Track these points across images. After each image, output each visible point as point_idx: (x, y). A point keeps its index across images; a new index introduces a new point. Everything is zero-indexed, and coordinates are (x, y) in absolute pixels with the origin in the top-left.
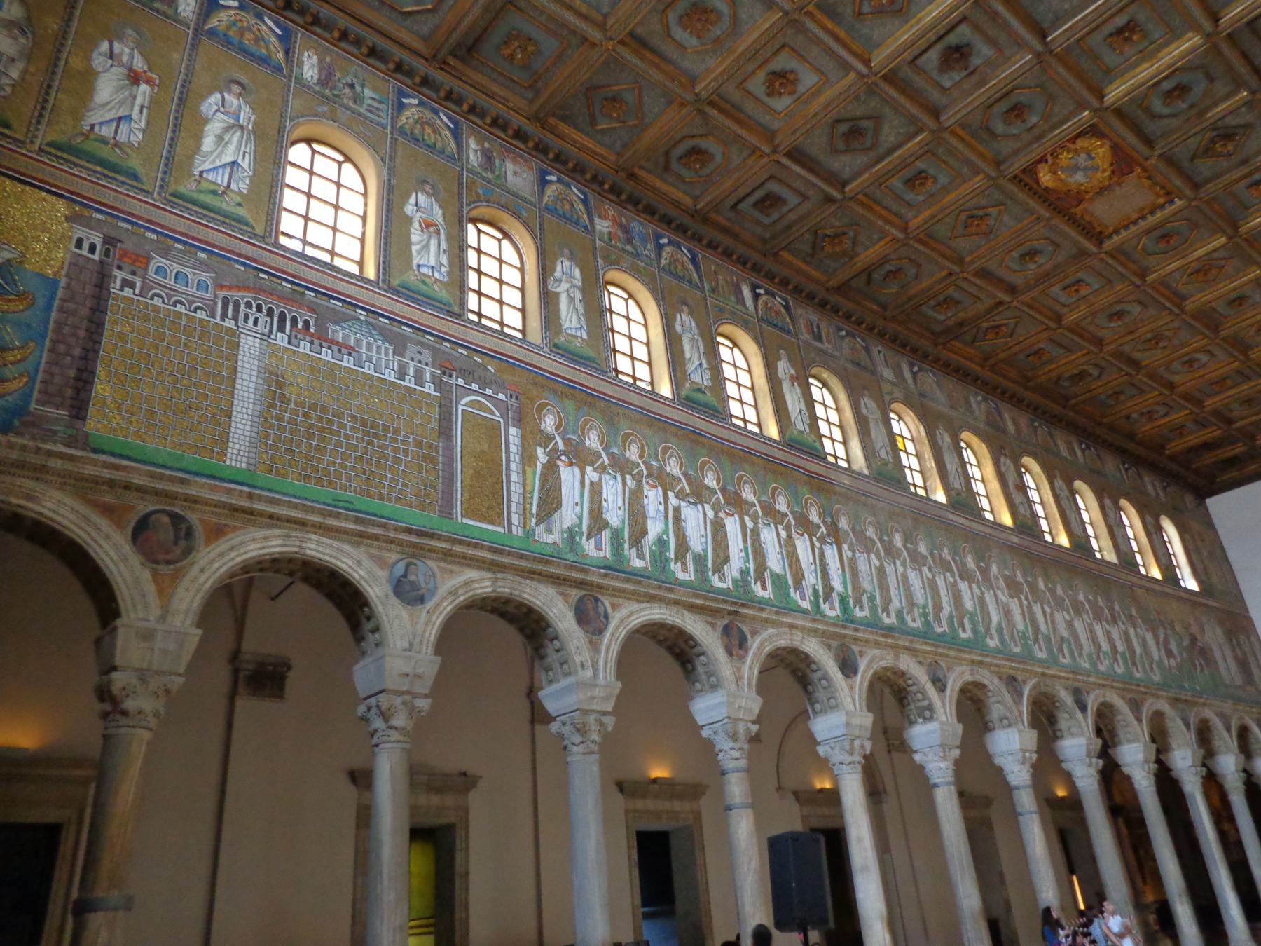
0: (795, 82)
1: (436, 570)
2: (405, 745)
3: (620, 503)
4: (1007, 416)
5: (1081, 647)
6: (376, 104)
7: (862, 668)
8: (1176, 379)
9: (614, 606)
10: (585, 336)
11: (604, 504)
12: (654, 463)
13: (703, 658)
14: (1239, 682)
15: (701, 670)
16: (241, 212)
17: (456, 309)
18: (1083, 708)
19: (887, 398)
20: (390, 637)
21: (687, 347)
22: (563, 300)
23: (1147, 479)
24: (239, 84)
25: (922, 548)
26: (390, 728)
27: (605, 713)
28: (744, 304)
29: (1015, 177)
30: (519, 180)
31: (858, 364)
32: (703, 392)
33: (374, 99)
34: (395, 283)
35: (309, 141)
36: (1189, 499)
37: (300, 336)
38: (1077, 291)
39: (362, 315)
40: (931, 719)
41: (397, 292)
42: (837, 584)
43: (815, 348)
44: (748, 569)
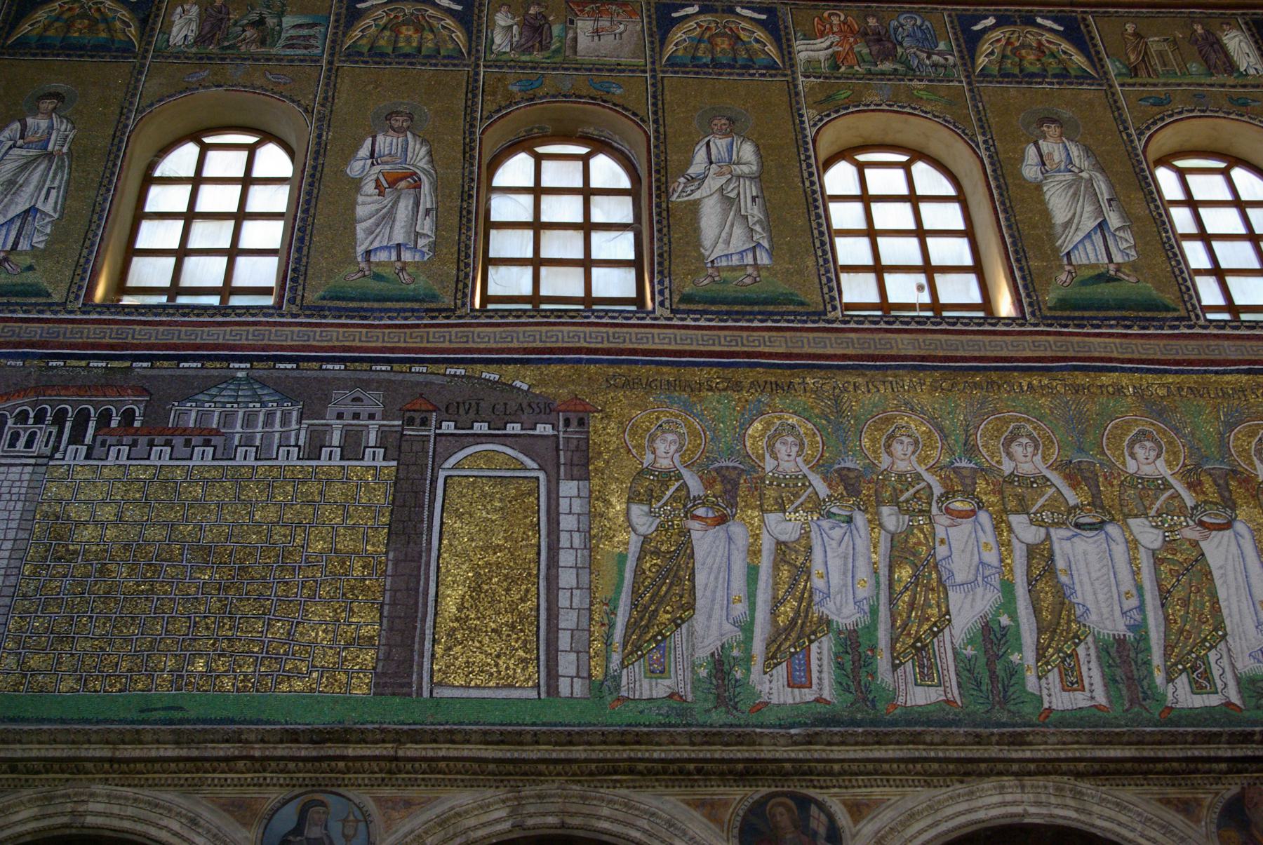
1: (371, 806)
3: (863, 572)
6: (305, 32)
10: (764, 259)
11: (818, 583)
12: (964, 464)
16: (30, 278)
17: (447, 301)
21: (1059, 204)
24: (57, 96)
28: (1231, 67)
30: (608, 41)
32: (1111, 279)
33: (300, 26)
34: (312, 297)
35: (195, 137)
37: (110, 440)
39: (240, 370)
41: (319, 310)
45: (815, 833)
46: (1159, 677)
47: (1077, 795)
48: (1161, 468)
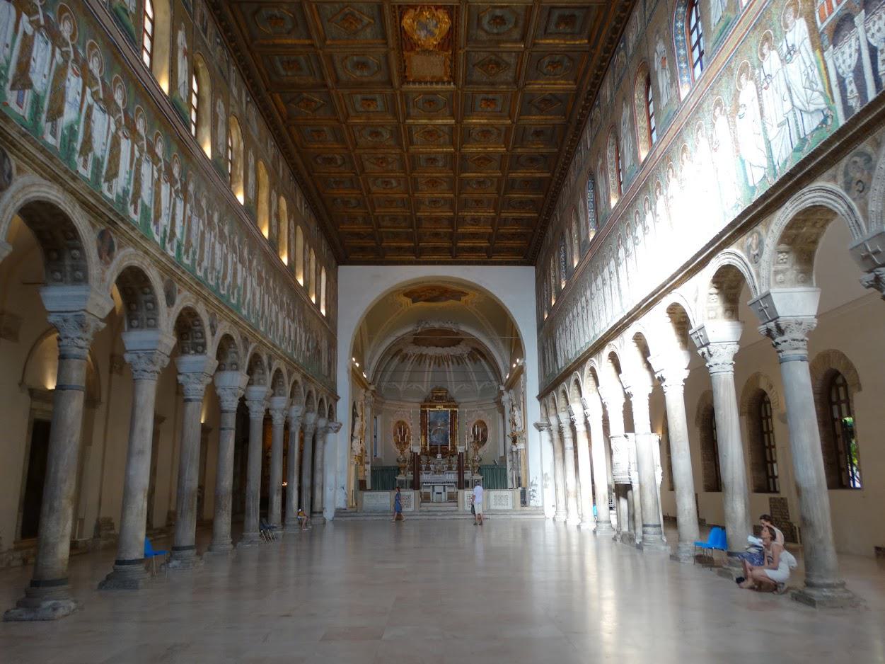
3: (46, 72)
4: (281, 164)
5: (278, 329)
7: (178, 300)
8: (374, 189)
9: (19, 170)
11: (32, 62)
13: (76, 252)
14: (326, 374)
15: (68, 262)
18: (270, 369)
19: (231, 109)
23: (323, 241)
25: (226, 231)
29: (394, 6)
31: (222, 72)
36: (334, 261)
38: (369, 105)
40: (202, 352)
42: (178, 231)
43: (202, 39)
44: (128, 190)
45: (4, 171)
46: (103, 180)
47: (74, 206)
48: (120, 102)
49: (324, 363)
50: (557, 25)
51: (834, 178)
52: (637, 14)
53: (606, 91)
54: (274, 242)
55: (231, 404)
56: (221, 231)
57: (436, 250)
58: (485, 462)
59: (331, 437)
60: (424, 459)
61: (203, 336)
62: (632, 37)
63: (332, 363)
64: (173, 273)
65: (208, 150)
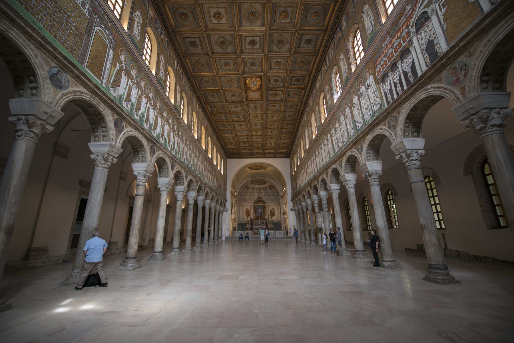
0: (221, 19)
1: (70, 80)
2: (36, 141)
8: (238, 134)
9: (126, 126)
15: (140, 155)
20: (43, 94)
22: (136, 23)
26: (31, 131)
27: (115, 157)
40: (183, 185)
42: (176, 146)
48: (158, 106)
49: (222, 190)
50: (294, 82)
51: (385, 125)
52: (319, 77)
53: (311, 102)
54: (206, 151)
55: (192, 202)
56: (190, 147)
57: (258, 153)
58: (274, 222)
59: (224, 213)
60: (255, 221)
61: (183, 180)
62: (318, 85)
63: (225, 189)
64: (174, 160)
65: (186, 122)
